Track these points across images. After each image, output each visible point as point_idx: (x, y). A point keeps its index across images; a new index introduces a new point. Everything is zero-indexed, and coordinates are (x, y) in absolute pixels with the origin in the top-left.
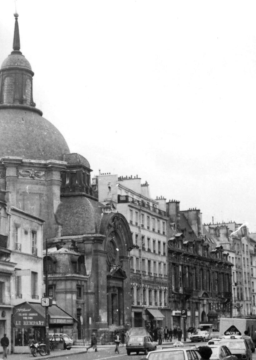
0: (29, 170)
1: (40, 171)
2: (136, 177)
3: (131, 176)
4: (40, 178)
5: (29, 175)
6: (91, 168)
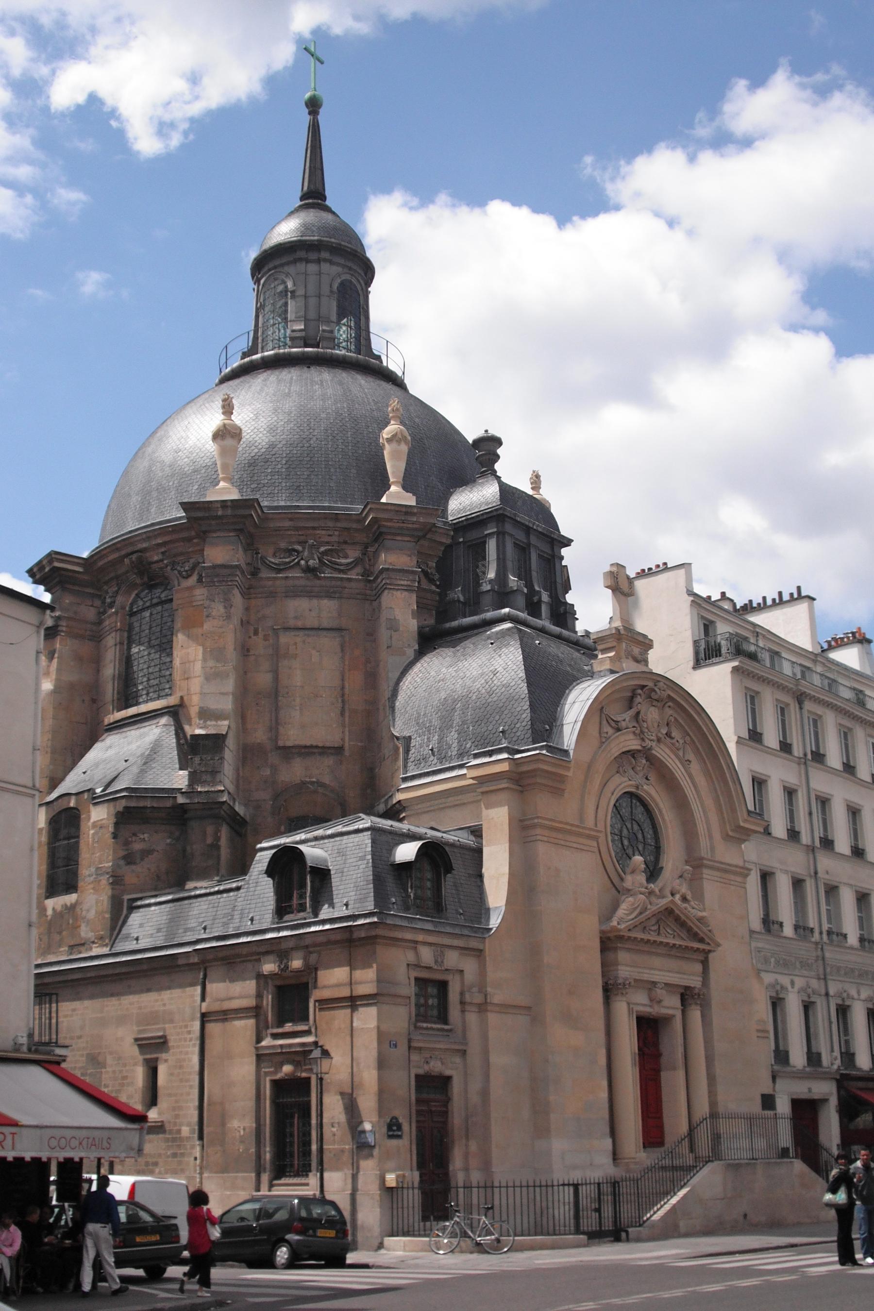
0: (300, 543)
1: (344, 546)
2: (796, 596)
3: (780, 593)
4: (340, 571)
5: (298, 563)
6: (565, 531)
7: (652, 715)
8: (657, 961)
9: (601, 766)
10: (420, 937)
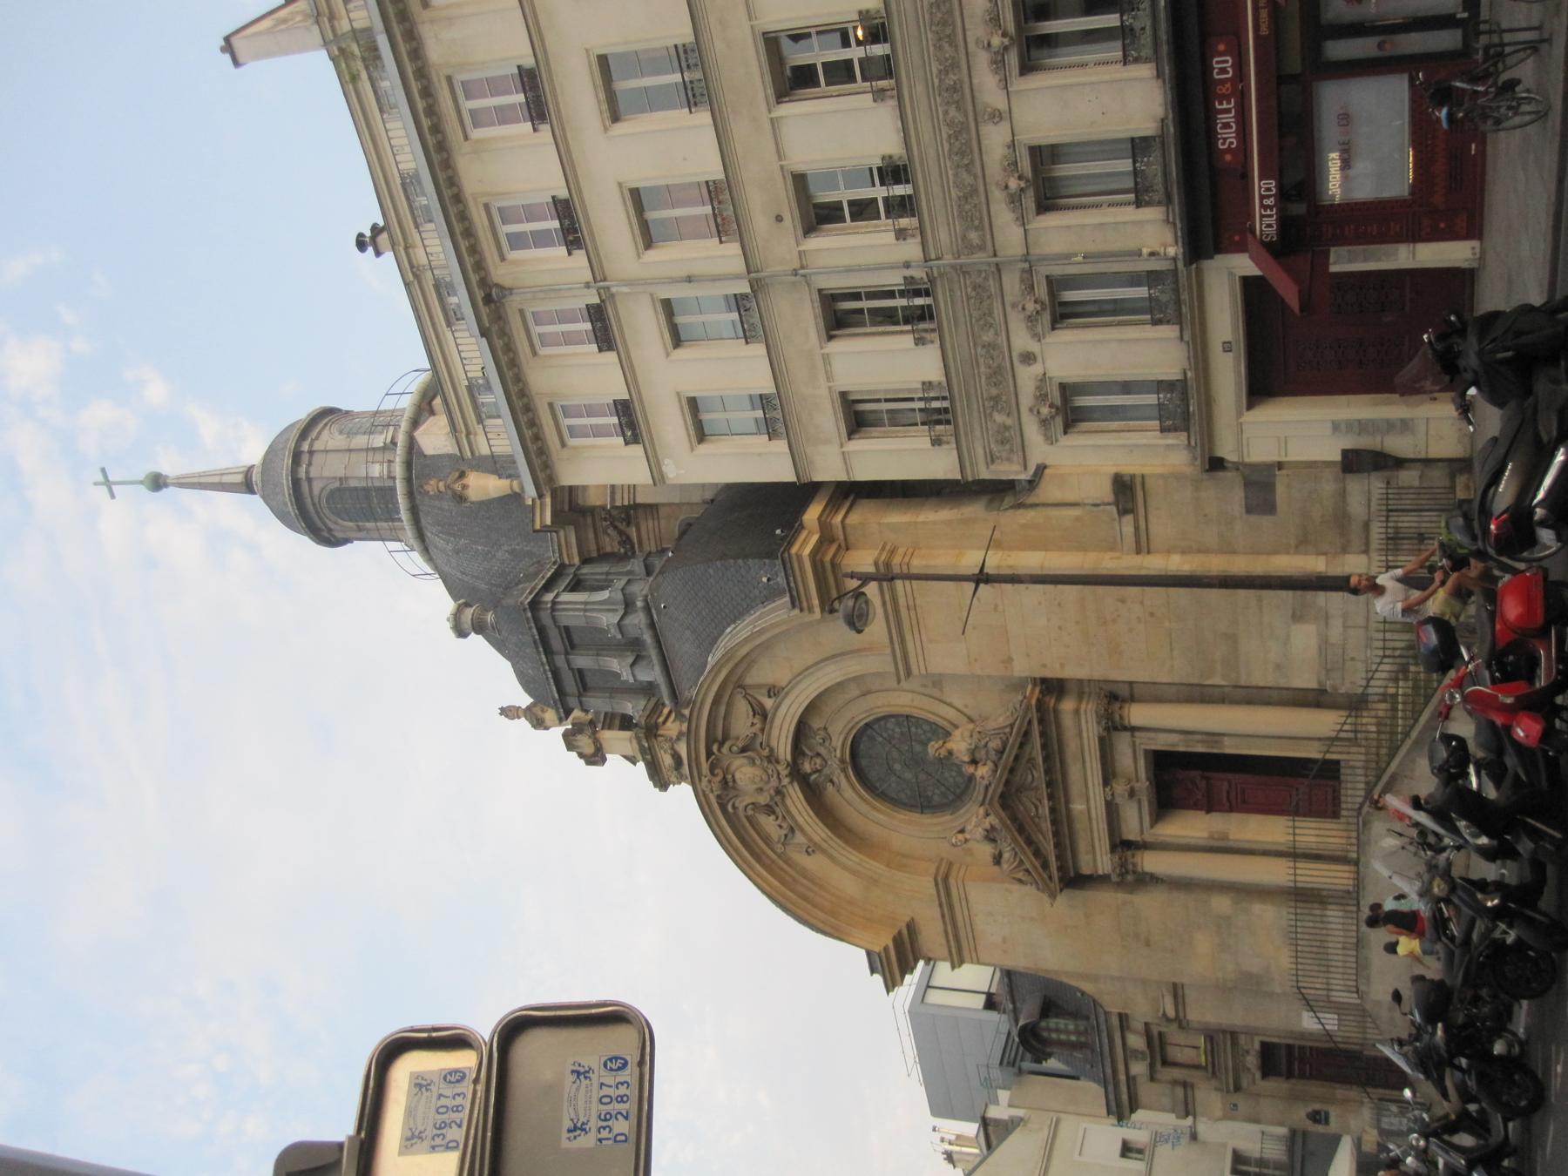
7: (746, 773)
8: (1078, 807)
9: (852, 857)
10: (1122, 1077)
